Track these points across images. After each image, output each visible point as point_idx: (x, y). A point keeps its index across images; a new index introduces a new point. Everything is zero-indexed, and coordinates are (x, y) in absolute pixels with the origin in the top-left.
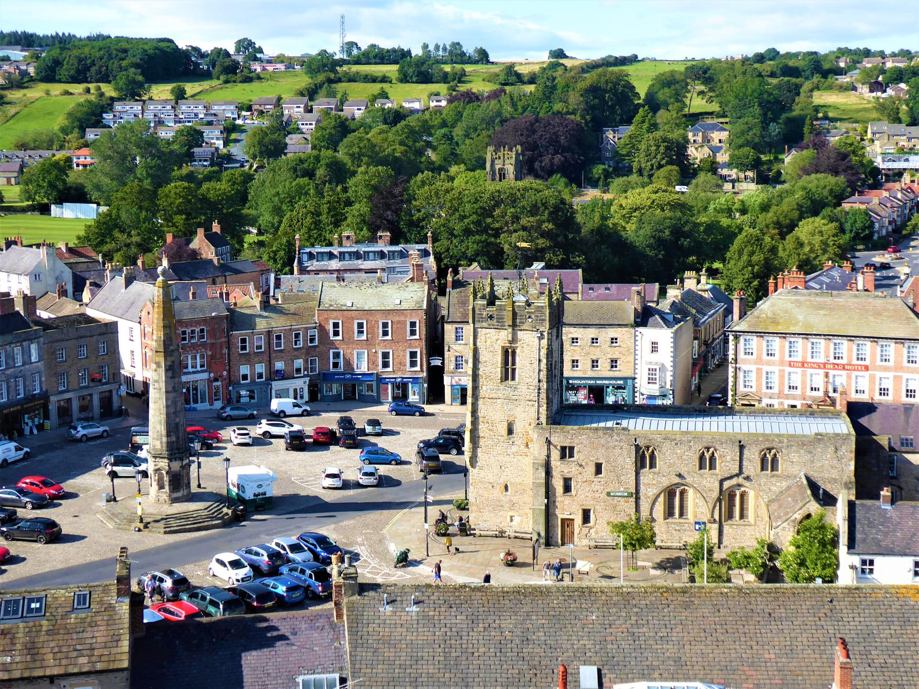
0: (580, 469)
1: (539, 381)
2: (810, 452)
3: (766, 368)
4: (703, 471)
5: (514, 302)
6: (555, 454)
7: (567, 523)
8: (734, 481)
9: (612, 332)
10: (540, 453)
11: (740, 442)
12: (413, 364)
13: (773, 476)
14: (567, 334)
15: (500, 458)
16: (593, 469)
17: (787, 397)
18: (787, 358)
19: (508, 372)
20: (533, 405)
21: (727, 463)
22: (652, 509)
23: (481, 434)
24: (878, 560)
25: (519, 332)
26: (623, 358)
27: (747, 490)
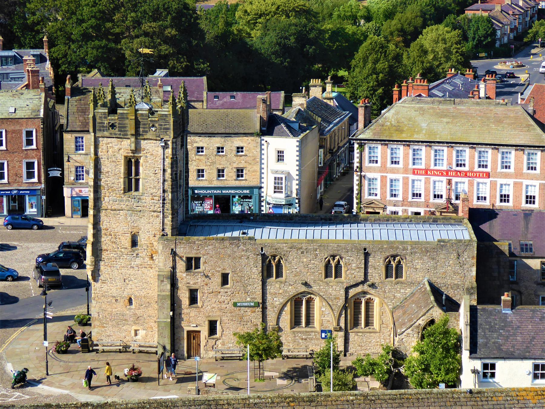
0: (206, 280)
1: (164, 191)
2: (433, 259)
3: (390, 176)
4: (329, 279)
5: (136, 111)
6: (181, 266)
7: (193, 335)
8: (359, 289)
9: (238, 142)
10: (165, 265)
11: (365, 249)
12: (30, 175)
14: (192, 143)
15: (124, 271)
16: (218, 279)
17: (411, 204)
18: (411, 166)
19: (131, 183)
20: (158, 216)
21: (352, 271)
22: (278, 318)
23: (104, 247)
24: (499, 364)
25: (142, 142)
26: (249, 167)
27: (372, 297)
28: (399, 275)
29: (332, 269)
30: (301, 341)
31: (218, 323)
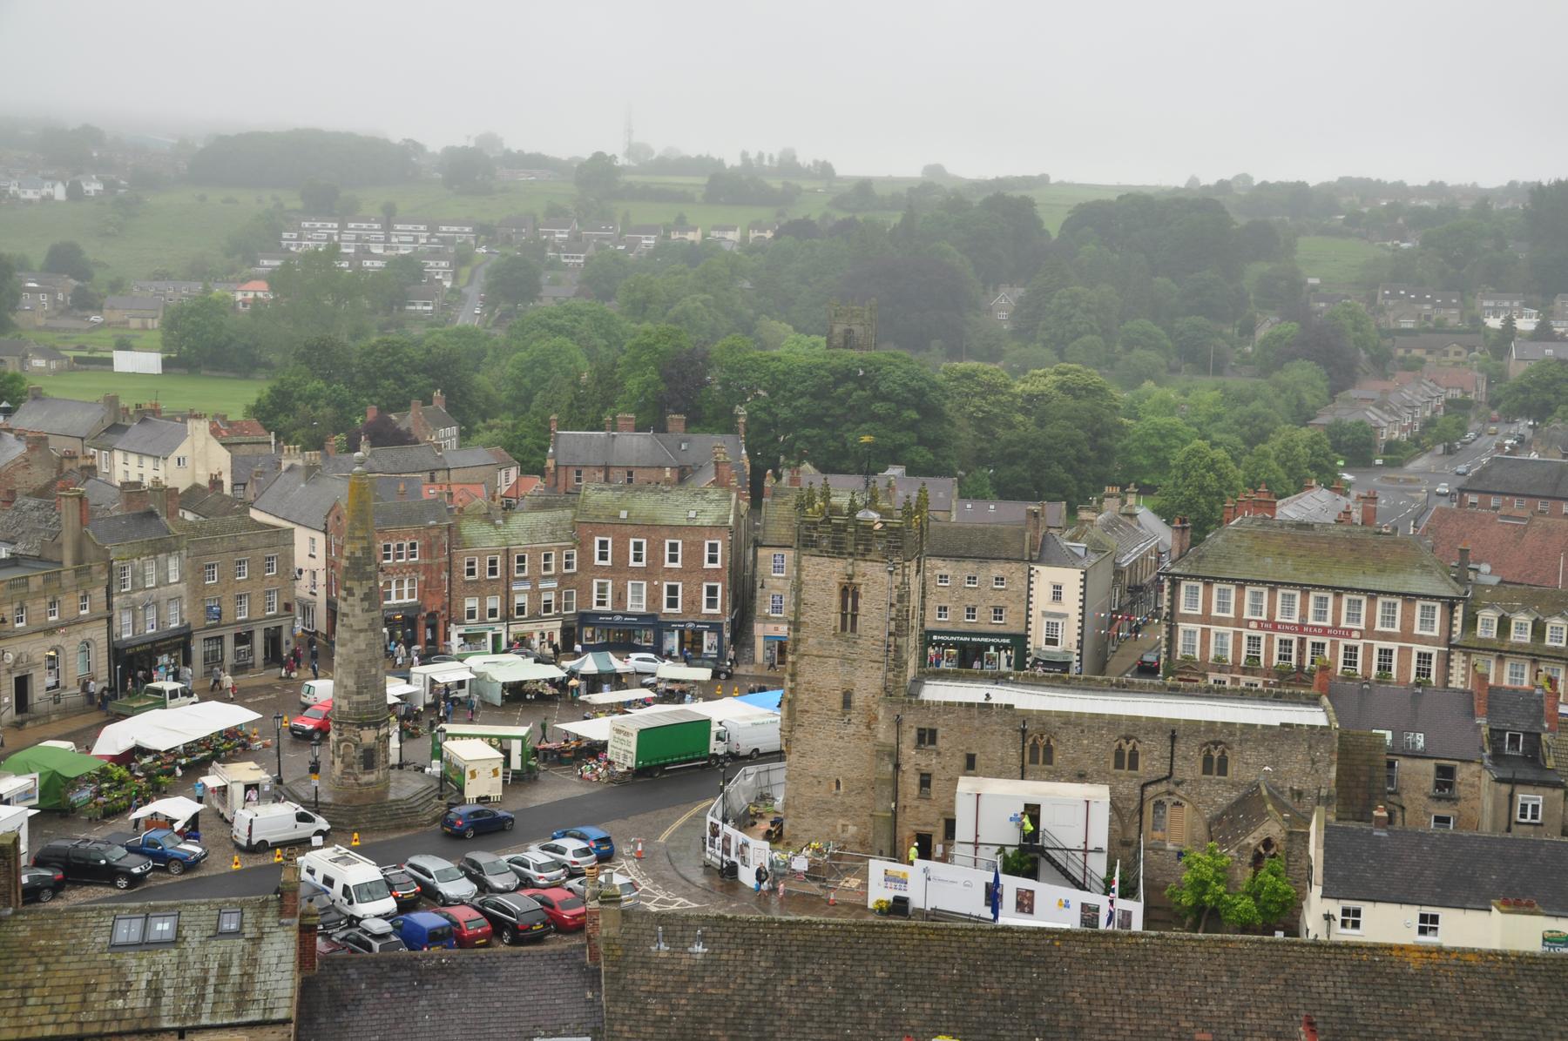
2: (1272, 751)
8: (1162, 787)
9: (997, 569)
12: (712, 603)
14: (932, 569)
17: (1244, 671)
21: (1151, 765)
24: (1367, 908)
26: (1011, 607)
28: (1223, 770)
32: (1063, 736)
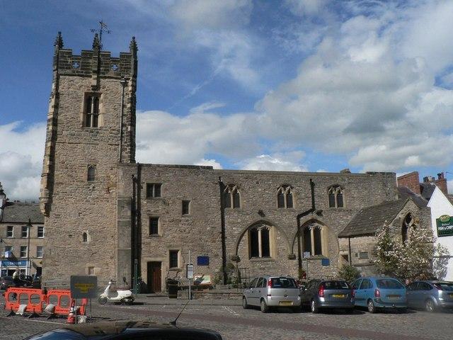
1: (123, 125)
5: (99, 52)
7: (154, 267)
8: (309, 217)
10: (125, 192)
11: (311, 180)
13: (340, 211)
16: (180, 208)
20: (115, 150)
28: (340, 204)
29: (284, 201)
30: (260, 271)
31: (179, 254)
32: (246, 185)
